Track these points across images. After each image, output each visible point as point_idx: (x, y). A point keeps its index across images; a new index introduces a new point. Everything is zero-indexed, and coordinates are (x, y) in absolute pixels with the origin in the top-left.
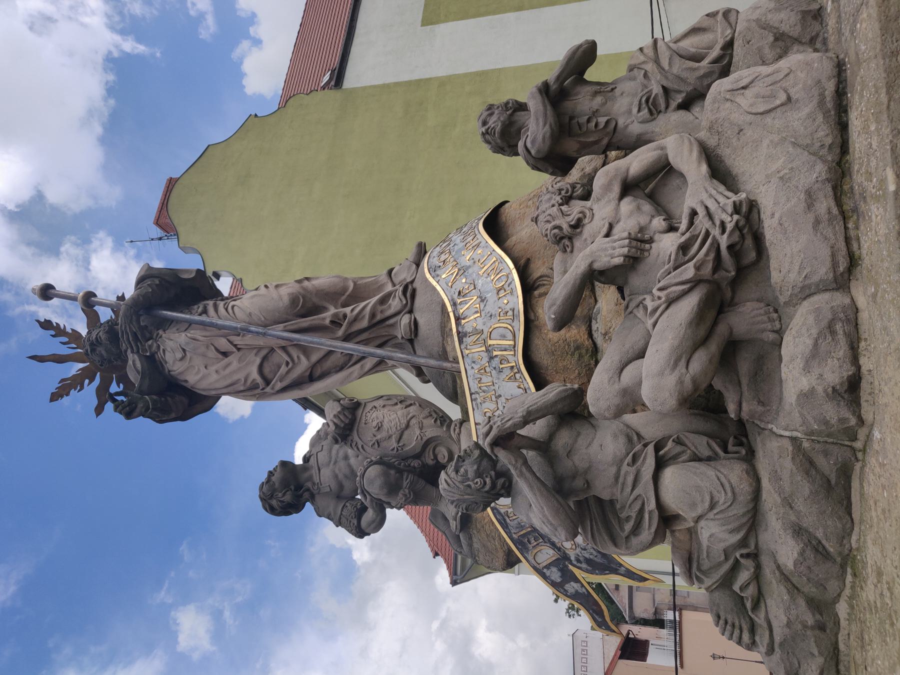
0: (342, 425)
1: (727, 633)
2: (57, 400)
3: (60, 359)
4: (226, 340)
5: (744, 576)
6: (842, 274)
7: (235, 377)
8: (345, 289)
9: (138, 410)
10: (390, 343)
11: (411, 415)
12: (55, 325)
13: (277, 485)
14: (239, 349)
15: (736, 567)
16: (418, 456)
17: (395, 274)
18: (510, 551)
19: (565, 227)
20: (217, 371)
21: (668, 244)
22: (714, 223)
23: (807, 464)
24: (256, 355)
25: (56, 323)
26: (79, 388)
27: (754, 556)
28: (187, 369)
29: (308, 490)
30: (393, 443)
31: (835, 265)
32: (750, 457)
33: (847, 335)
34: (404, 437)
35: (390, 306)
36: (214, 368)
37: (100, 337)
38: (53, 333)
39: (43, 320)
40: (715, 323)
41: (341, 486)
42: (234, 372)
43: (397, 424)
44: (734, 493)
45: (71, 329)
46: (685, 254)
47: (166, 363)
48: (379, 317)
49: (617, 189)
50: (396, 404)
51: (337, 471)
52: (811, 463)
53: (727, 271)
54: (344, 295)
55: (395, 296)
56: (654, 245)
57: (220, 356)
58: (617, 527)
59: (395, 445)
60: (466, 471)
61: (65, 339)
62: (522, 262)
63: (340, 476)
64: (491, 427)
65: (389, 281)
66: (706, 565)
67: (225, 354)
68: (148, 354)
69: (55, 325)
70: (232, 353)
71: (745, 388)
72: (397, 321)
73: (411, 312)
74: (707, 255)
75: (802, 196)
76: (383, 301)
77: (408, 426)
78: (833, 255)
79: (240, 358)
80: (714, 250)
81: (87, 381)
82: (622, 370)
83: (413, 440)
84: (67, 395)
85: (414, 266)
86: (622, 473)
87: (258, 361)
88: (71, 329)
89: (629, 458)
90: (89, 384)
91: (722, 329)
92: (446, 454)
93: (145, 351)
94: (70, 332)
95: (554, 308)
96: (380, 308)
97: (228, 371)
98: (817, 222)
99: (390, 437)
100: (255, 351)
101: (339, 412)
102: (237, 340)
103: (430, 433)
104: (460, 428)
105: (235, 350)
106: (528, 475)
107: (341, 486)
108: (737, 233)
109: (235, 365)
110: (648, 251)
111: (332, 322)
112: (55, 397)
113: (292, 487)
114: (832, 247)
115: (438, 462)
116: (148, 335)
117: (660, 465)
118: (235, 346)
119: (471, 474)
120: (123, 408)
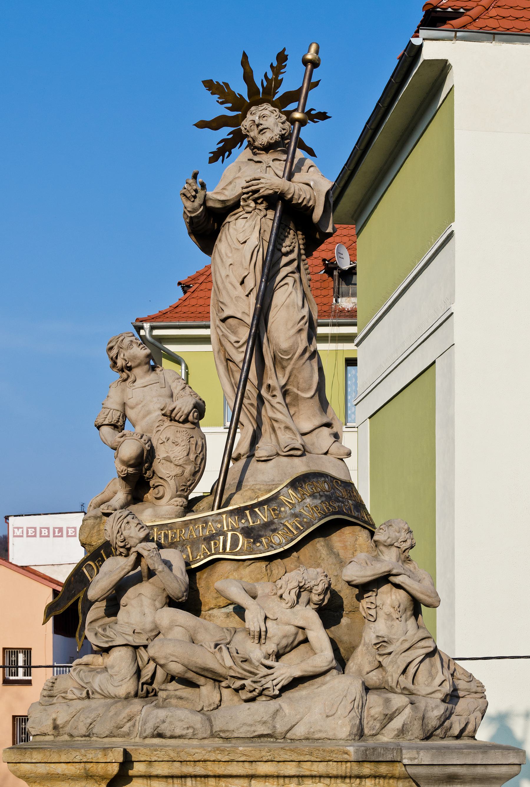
2: (205, 87)
3: (248, 77)
4: (252, 287)
6: (219, 734)
7: (224, 292)
12: (283, 64)
14: (247, 296)
22: (262, 677)
25: (286, 65)
31: (224, 731)
39: (286, 53)
43: (177, 457)
45: (282, 79)
46: (242, 661)
47: (237, 219)
48: (276, 425)
52: (129, 720)
54: (298, 390)
57: (240, 280)
61: (270, 75)
67: (242, 283)
68: (242, 203)
70: (244, 289)
74: (239, 673)
75: (264, 719)
78: (228, 731)
80: (243, 677)
81: (230, 105)
87: (239, 315)
88: (282, 79)
90: (228, 108)
93: (245, 200)
94: (280, 78)
97: (229, 287)
105: (247, 293)
108: (252, 689)
112: (209, 85)
114: (233, 731)
116: (259, 201)
118: (249, 293)
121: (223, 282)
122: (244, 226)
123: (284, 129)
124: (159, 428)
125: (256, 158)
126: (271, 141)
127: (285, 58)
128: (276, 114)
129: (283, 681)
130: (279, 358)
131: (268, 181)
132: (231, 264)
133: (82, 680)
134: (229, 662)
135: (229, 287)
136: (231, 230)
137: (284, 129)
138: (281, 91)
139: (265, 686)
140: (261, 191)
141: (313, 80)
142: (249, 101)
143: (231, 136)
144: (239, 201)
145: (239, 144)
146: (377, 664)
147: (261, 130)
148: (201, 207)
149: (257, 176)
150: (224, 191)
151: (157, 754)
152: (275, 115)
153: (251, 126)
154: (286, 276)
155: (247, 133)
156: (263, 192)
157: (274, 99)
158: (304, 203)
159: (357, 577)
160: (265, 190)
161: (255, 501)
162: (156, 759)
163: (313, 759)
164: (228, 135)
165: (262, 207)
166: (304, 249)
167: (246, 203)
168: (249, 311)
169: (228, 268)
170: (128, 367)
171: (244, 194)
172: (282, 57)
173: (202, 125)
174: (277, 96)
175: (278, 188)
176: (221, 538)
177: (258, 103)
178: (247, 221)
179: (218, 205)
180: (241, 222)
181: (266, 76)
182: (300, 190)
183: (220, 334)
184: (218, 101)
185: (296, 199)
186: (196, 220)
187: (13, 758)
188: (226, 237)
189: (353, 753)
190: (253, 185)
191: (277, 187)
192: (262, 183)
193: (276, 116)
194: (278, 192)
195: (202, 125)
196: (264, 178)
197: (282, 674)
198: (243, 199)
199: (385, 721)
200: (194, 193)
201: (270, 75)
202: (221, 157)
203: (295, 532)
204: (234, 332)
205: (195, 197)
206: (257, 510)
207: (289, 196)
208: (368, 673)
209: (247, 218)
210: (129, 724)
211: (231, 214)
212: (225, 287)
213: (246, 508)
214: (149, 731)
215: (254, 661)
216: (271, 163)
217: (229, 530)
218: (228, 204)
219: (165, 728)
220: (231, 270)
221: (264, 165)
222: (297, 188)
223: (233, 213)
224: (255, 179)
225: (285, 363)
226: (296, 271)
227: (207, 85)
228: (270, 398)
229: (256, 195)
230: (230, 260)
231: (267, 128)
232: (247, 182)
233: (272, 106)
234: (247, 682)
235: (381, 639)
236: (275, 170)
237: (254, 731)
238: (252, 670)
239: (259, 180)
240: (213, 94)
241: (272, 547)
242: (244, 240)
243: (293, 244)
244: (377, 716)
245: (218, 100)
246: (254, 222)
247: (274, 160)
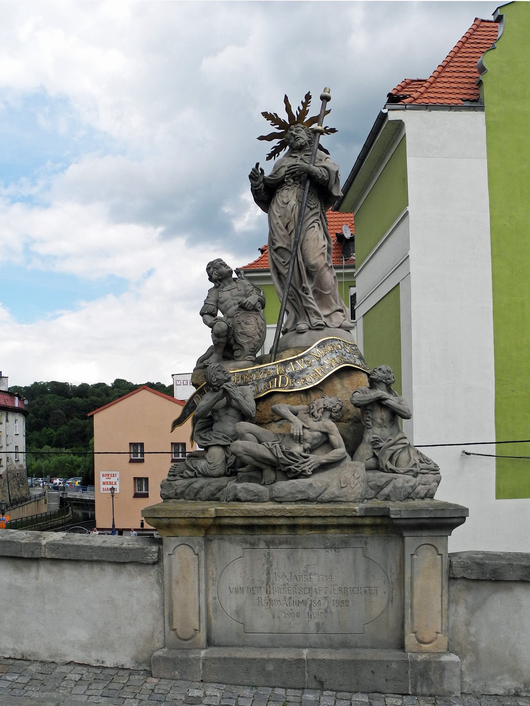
0: (246, 306)
1: (172, 468)
2: (263, 116)
3: (288, 109)
5: (190, 473)
7: (275, 233)
8: (325, 290)
9: (254, 182)
10: (297, 315)
11: (254, 337)
12: (309, 101)
13: (220, 270)
14: (290, 235)
15: (192, 471)
16: (235, 342)
17: (336, 314)
18: (199, 386)
19: (312, 411)
21: (297, 449)
22: (301, 464)
23: (220, 489)
24: (287, 245)
27: (196, 476)
28: (278, 205)
29: (220, 285)
30: (240, 330)
31: (278, 497)
32: (225, 475)
33: (254, 500)
34: (243, 335)
35: (313, 317)
36: (280, 221)
37: (299, 140)
38: (304, 101)
39: (310, 95)
40: (266, 464)
41: (222, 303)
42: (278, 233)
44: (214, 469)
46: (289, 454)
47: (283, 190)
49: (324, 430)
50: (259, 329)
51: (228, 301)
52: (220, 491)
53: (284, 468)
55: (319, 319)
56: (298, 444)
57: (285, 225)
58: (204, 432)
59: (239, 331)
60: (218, 375)
62: (322, 388)
63: (226, 303)
64: (230, 387)
65: (332, 312)
66: (193, 461)
67: (286, 227)
68: (285, 181)
69: (309, 101)
71: (246, 473)
72: (306, 321)
73: (310, 329)
74: (287, 461)
75: (302, 490)
76: (316, 313)
77: (249, 336)
79: (285, 236)
80: (289, 464)
81: (278, 126)
82: (250, 433)
83: (242, 340)
84: (267, 120)
85: (338, 326)
86: (220, 434)
87: (285, 246)
89: (225, 436)
91: (263, 466)
92: (237, 355)
93: (287, 179)
94: (307, 109)
95: (278, 408)
96: (312, 312)
97: (278, 229)
98: (293, 494)
99: (243, 329)
100: (289, 243)
101: (251, 304)
102: (293, 236)
103: (246, 347)
104: (250, 360)
105: (289, 233)
106: (214, 401)
107: (222, 303)
108: (295, 471)
109: (282, 233)
110: (296, 442)
111: (304, 287)
112: (265, 114)
113: (219, 278)
115: (234, 351)
116: (296, 179)
117: (224, 447)
118: (291, 233)
119: (218, 377)
120: (254, 175)
121: (275, 227)
124: (237, 315)
125: (294, 155)
129: (314, 466)
130: (309, 271)
132: (280, 216)
133: (193, 466)
134: (281, 455)
135: (278, 229)
138: (308, 117)
139: (303, 469)
141: (327, 109)
143: (279, 144)
144: (284, 179)
146: (372, 454)
147: (297, 138)
151: (236, 512)
154: (313, 222)
159: (359, 401)
161: (296, 357)
162: (235, 515)
163: (333, 515)
164: (278, 143)
166: (324, 207)
168: (291, 243)
170: (219, 279)
172: (308, 97)
173: (261, 138)
174: (305, 120)
176: (276, 379)
180: (285, 191)
183: (274, 258)
184: (271, 124)
187: (147, 514)
189: (358, 511)
195: (261, 138)
197: (313, 462)
199: (378, 490)
201: (301, 108)
202: (273, 157)
203: (321, 375)
204: (282, 257)
206: (297, 361)
208: (367, 460)
210: (220, 493)
212: (276, 230)
213: (290, 361)
214: (231, 497)
215: (296, 454)
217: (281, 374)
219: (241, 495)
224: (293, 165)
225: (313, 274)
228: (305, 295)
231: (300, 137)
234: (290, 467)
235: (375, 439)
237: (297, 497)
238: (295, 459)
240: (267, 120)
241: (307, 384)
244: (373, 487)
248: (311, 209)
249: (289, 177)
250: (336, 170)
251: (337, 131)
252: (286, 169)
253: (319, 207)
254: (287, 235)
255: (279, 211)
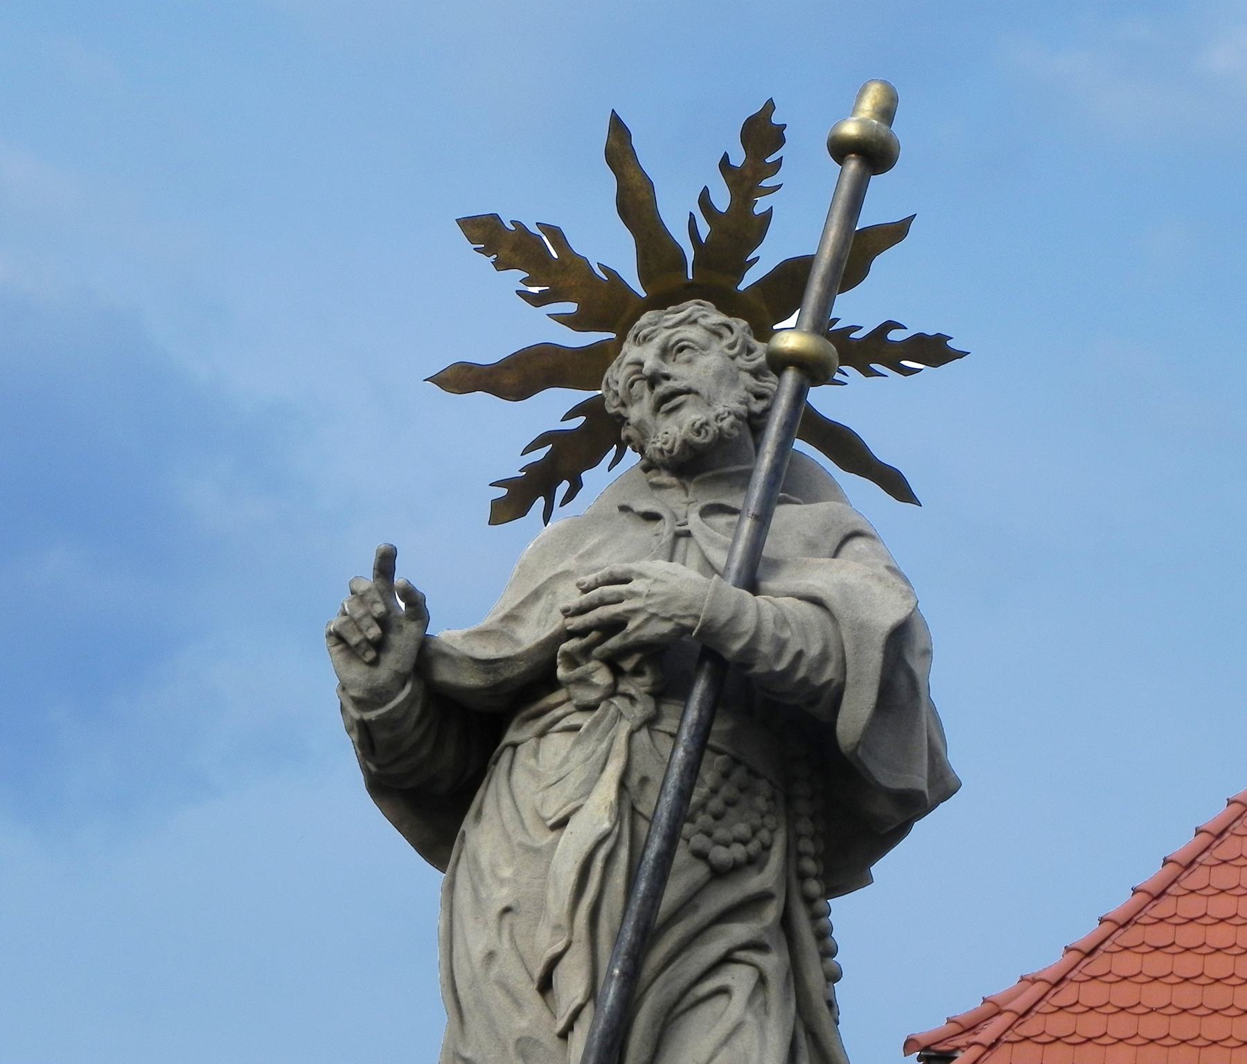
4: (579, 1001)
14: (564, 1035)
20: (491, 956)
26: (535, 290)
42: (491, 1023)
47: (542, 734)
57: (538, 972)
67: (545, 985)
68: (561, 672)
81: (570, 307)
94: (759, 209)
97: (498, 999)
105: (561, 1024)
116: (628, 665)
122: (566, 760)
123: (759, 396)
126: (698, 439)
127: (776, 137)
128: (730, 339)
131: (657, 588)
132: (507, 910)
136: (519, 775)
137: (759, 396)
140: (631, 626)
142: (644, 295)
145: (611, 454)
148: (403, 686)
149: (619, 568)
150: (512, 625)
152: (725, 342)
153: (632, 385)
155: (622, 410)
156: (638, 628)
157: (741, 287)
158: (801, 673)
160: (647, 621)
164: (569, 416)
165: (637, 686)
167: (578, 672)
169: (493, 924)
171: (572, 634)
174: (751, 277)
175: (694, 611)
177: (662, 300)
178: (577, 743)
179: (470, 679)
180: (557, 744)
181: (705, 200)
182: (782, 621)
184: (522, 294)
185: (766, 657)
186: (382, 736)
188: (498, 801)
190: (603, 602)
191: (686, 608)
192: (633, 594)
193: (731, 347)
194: (691, 629)
196: (641, 575)
198: (566, 654)
200: (374, 632)
202: (540, 502)
205: (379, 645)
207: (737, 646)
209: (576, 728)
211: (525, 714)
216: (694, 521)
218: (507, 674)
220: (506, 932)
221: (665, 529)
222: (768, 615)
223: (534, 709)
226: (767, 940)
227: (478, 233)
229: (614, 642)
230: (505, 891)
231: (688, 391)
232: (585, 591)
233: (721, 308)
236: (704, 547)
239: (627, 581)
240: (500, 265)
242: (561, 814)
243: (764, 834)
245: (523, 287)
246: (604, 745)
247: (709, 511)
248: (720, 874)
249: (586, 652)
250: (888, 615)
251: (961, 354)
252: (576, 599)
253: (776, 858)
254: (549, 1039)
255: (507, 872)
